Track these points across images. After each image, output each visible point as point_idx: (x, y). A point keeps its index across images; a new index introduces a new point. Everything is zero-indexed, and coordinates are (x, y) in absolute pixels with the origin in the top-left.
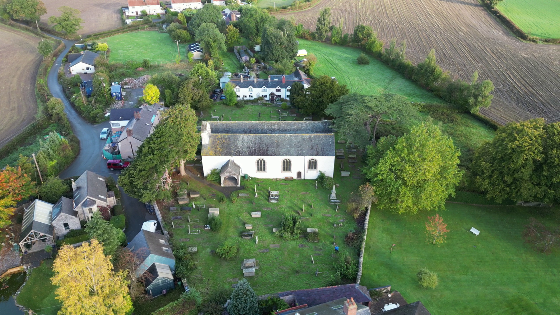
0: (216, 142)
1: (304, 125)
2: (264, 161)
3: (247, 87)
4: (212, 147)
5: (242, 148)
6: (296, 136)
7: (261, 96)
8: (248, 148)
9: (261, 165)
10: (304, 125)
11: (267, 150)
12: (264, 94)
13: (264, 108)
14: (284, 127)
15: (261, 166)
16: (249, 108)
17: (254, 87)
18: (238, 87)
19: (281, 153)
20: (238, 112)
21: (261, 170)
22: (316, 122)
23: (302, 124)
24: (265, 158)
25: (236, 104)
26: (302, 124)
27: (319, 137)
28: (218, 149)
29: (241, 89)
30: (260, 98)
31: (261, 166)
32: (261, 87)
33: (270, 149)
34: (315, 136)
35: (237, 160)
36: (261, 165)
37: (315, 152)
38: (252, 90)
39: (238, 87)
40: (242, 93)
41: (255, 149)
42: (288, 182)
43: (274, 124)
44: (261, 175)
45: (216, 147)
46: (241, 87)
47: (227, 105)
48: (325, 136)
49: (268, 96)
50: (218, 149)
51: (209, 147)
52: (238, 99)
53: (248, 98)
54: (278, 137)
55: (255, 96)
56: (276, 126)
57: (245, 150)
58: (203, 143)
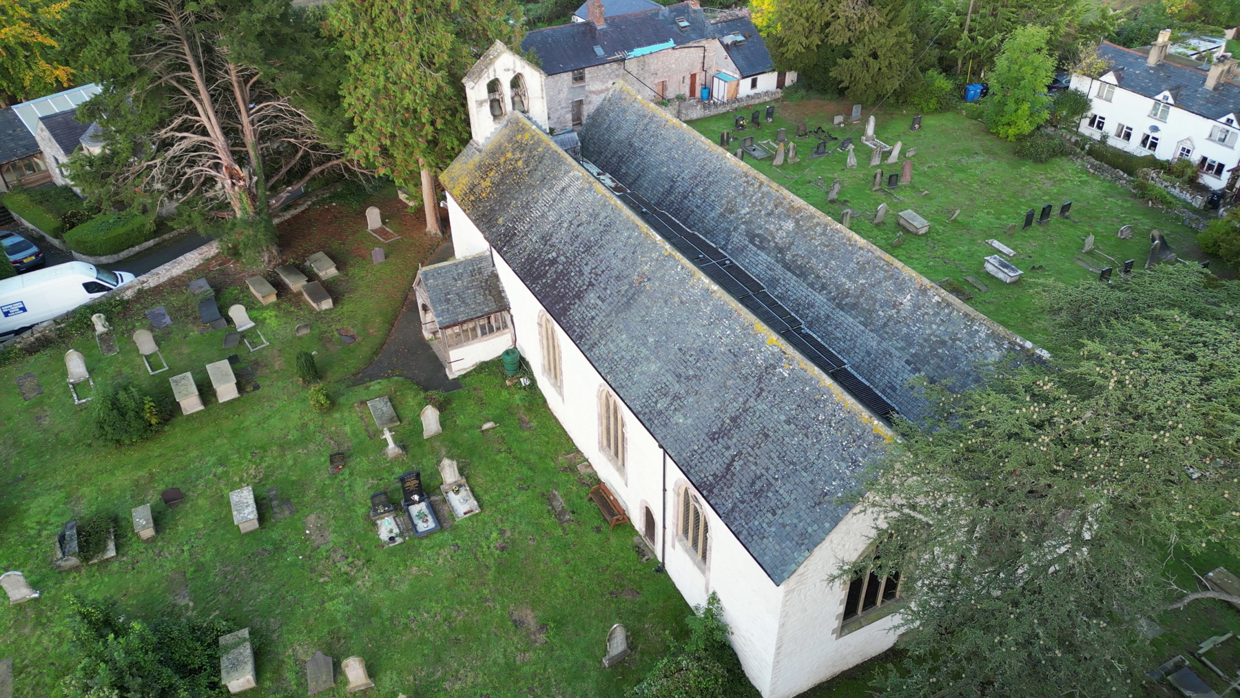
1: (906, 300)
3: (1148, 93)
4: (480, 167)
5: (533, 223)
6: (723, 313)
7: (1195, 158)
8: (545, 239)
10: (906, 300)
12: (1216, 154)
13: (1115, 204)
14: (812, 253)
16: (1067, 180)
17: (1179, 103)
18: (1110, 78)
20: (991, 168)
22: (984, 327)
23: (901, 287)
25: (1020, 138)
26: (901, 287)
27: (816, 400)
29: (1121, 94)
30: (1186, 172)
32: (1215, 117)
33: (591, 298)
34: (796, 378)
37: (716, 466)
38: (1163, 119)
39: (1110, 78)
40: (1120, 111)
41: (553, 262)
42: (590, 511)
43: (791, 212)
46: (1123, 83)
47: (989, 126)
48: (852, 415)
49: (1226, 175)
51: (477, 158)
52: (1085, 128)
53: (1134, 147)
54: (662, 262)
55: (1165, 152)
56: (790, 225)
57: (529, 243)
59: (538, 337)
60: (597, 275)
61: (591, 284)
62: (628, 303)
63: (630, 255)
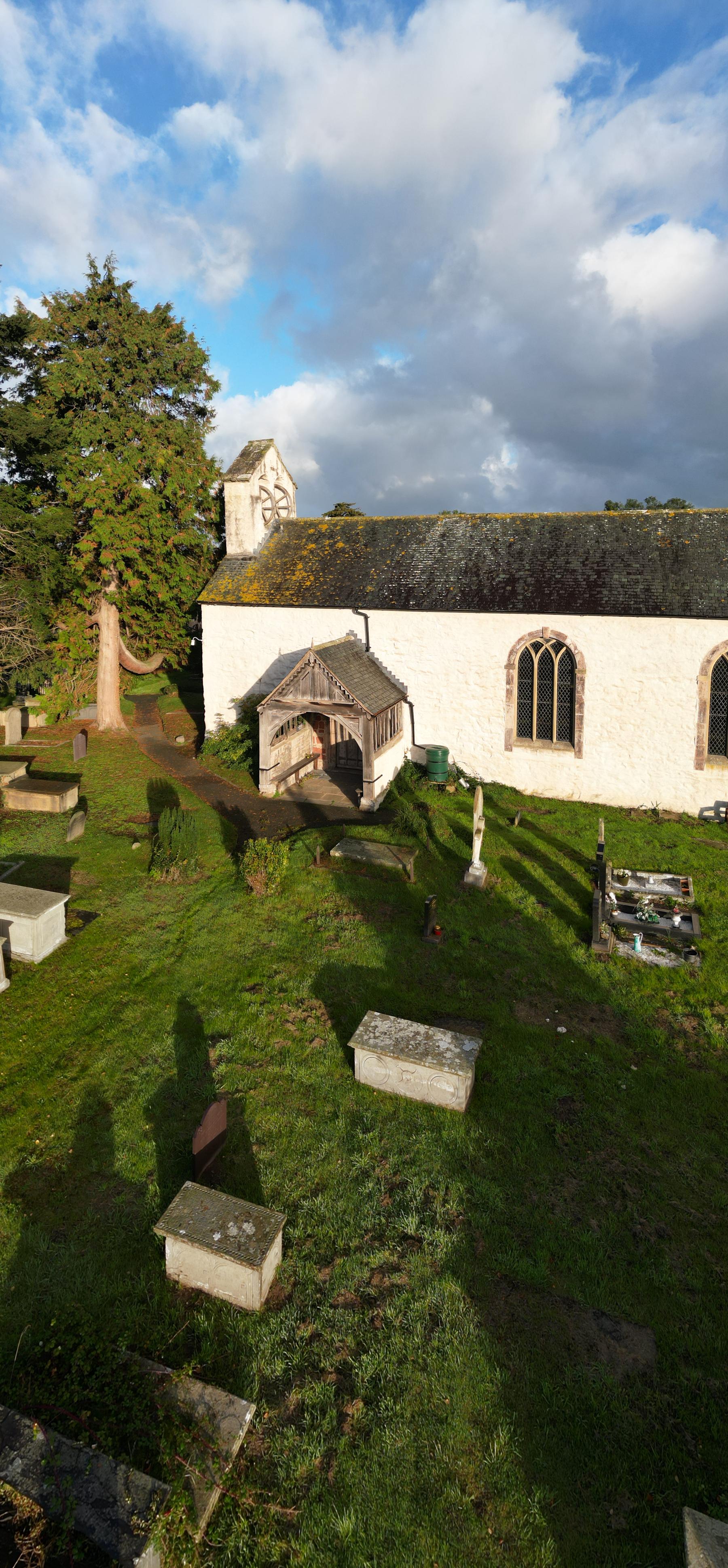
0: (298, 548)
2: (570, 660)
8: (472, 570)
9: (546, 691)
11: (592, 586)
15: (548, 700)
19: (702, 604)
21: (545, 733)
24: (582, 632)
28: (299, 575)
31: (548, 700)
33: (618, 578)
35: (399, 638)
36: (546, 691)
44: (539, 772)
45: (288, 568)
50: (299, 575)
51: (251, 569)
58: (232, 549)
59: (504, 686)
60: (598, 563)
61: (598, 573)
62: (676, 560)
63: (622, 535)
